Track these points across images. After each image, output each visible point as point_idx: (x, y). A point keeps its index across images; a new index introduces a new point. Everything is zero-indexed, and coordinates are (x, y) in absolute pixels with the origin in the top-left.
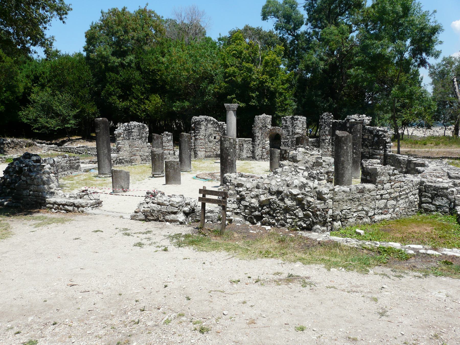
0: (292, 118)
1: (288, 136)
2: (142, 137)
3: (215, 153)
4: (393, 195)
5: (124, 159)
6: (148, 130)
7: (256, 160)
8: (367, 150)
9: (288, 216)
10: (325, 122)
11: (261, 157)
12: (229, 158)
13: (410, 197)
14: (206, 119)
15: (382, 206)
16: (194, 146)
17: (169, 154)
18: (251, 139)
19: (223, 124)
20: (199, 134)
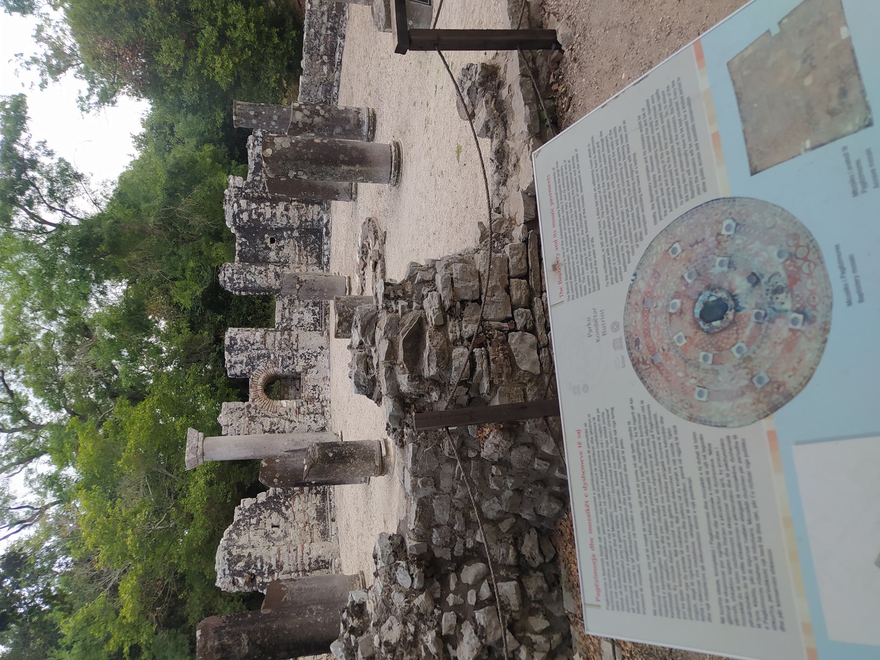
0: (231, 349)
1: (269, 357)
3: (316, 522)
19: (240, 509)
20: (265, 559)
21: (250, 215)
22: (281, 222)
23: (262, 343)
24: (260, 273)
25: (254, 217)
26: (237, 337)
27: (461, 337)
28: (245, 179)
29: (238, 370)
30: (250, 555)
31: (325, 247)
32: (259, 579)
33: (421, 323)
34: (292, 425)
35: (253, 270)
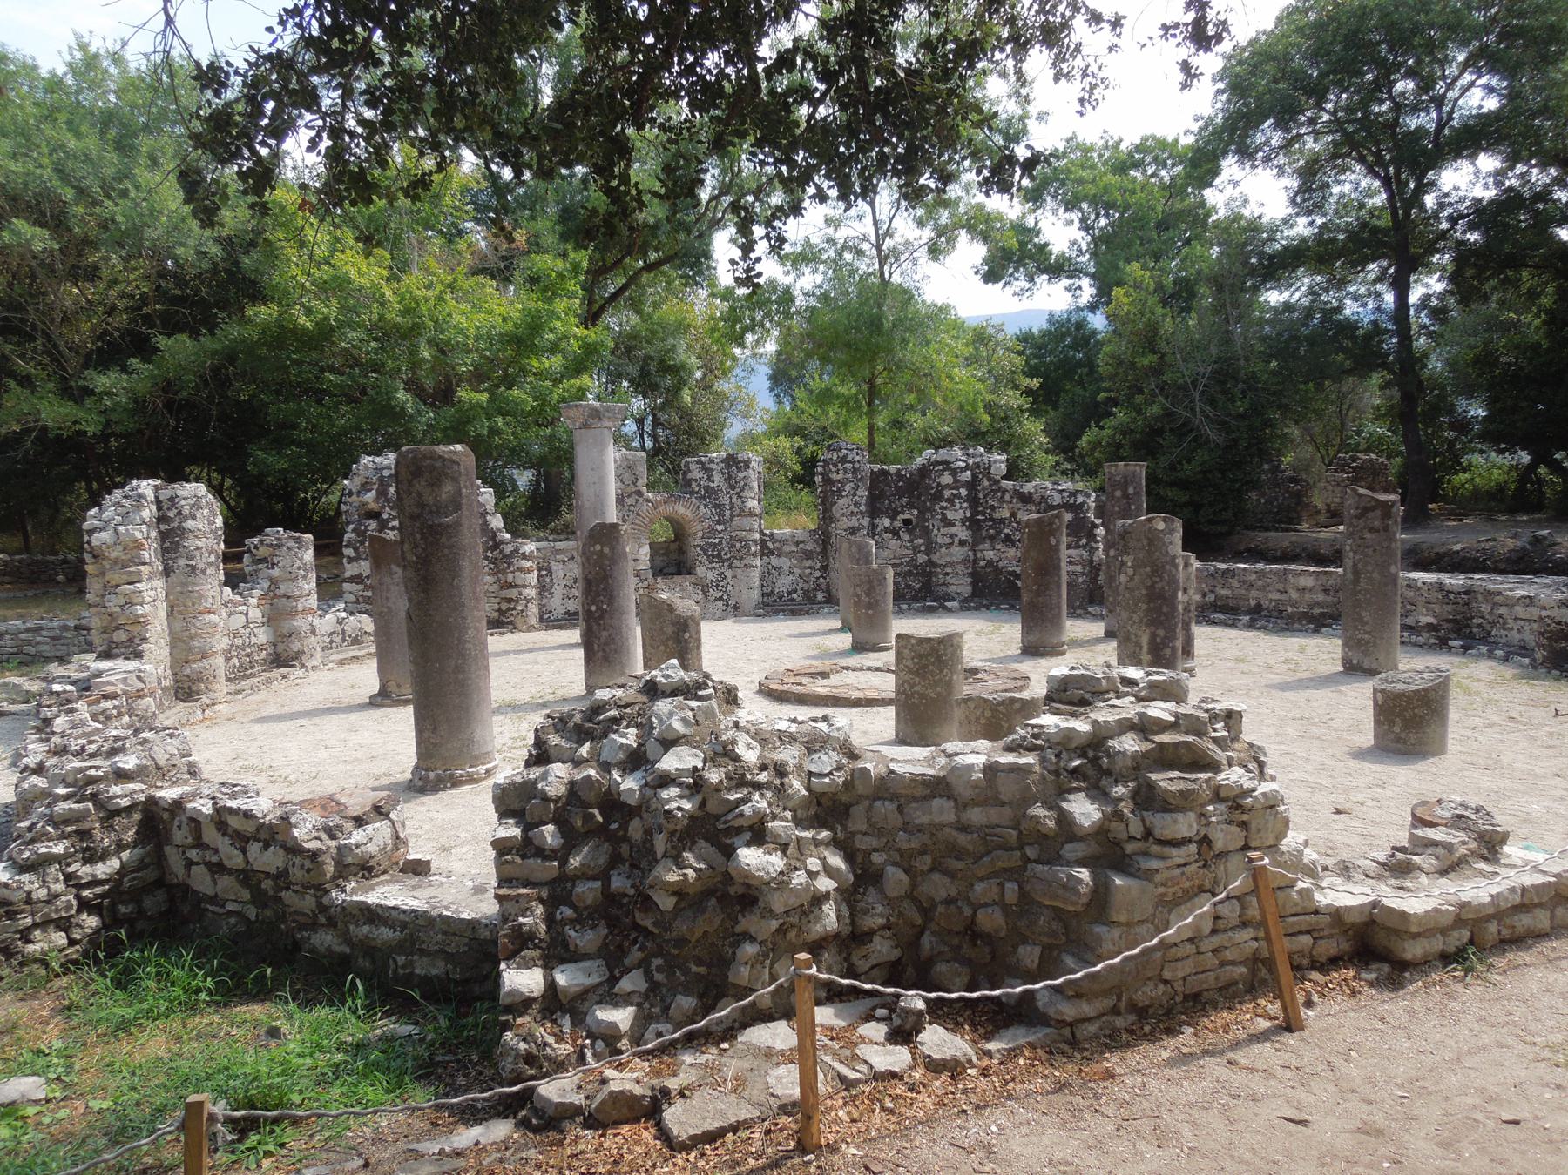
1: (718, 522)
8: (1012, 552)
21: (948, 486)
22: (939, 535)
23: (742, 510)
24: (856, 504)
25: (947, 493)
27: (1209, 824)
28: (1005, 478)
29: (696, 473)
31: (905, 606)
33: (1214, 767)
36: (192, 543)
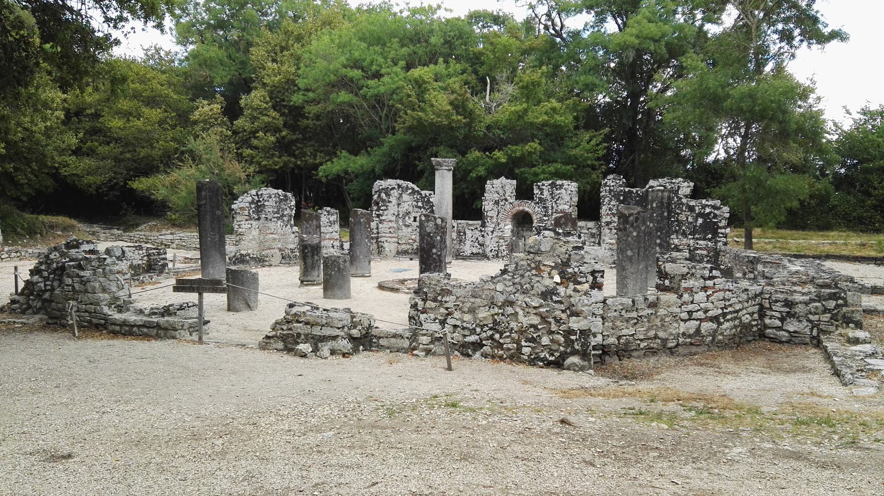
0: (553, 185)
1: (545, 216)
2: (283, 215)
4: (710, 314)
5: (249, 255)
6: (293, 203)
7: (488, 259)
8: (685, 241)
9: (523, 343)
10: (610, 191)
11: (497, 255)
12: (434, 251)
13: (743, 318)
14: (399, 186)
15: (691, 331)
16: (378, 233)
17: (333, 247)
18: (480, 222)
24: (610, 209)
26: (563, 191)
29: (536, 191)
30: (390, 202)
32: (375, 208)
34: (490, 233)
35: (613, 203)
36: (267, 210)
